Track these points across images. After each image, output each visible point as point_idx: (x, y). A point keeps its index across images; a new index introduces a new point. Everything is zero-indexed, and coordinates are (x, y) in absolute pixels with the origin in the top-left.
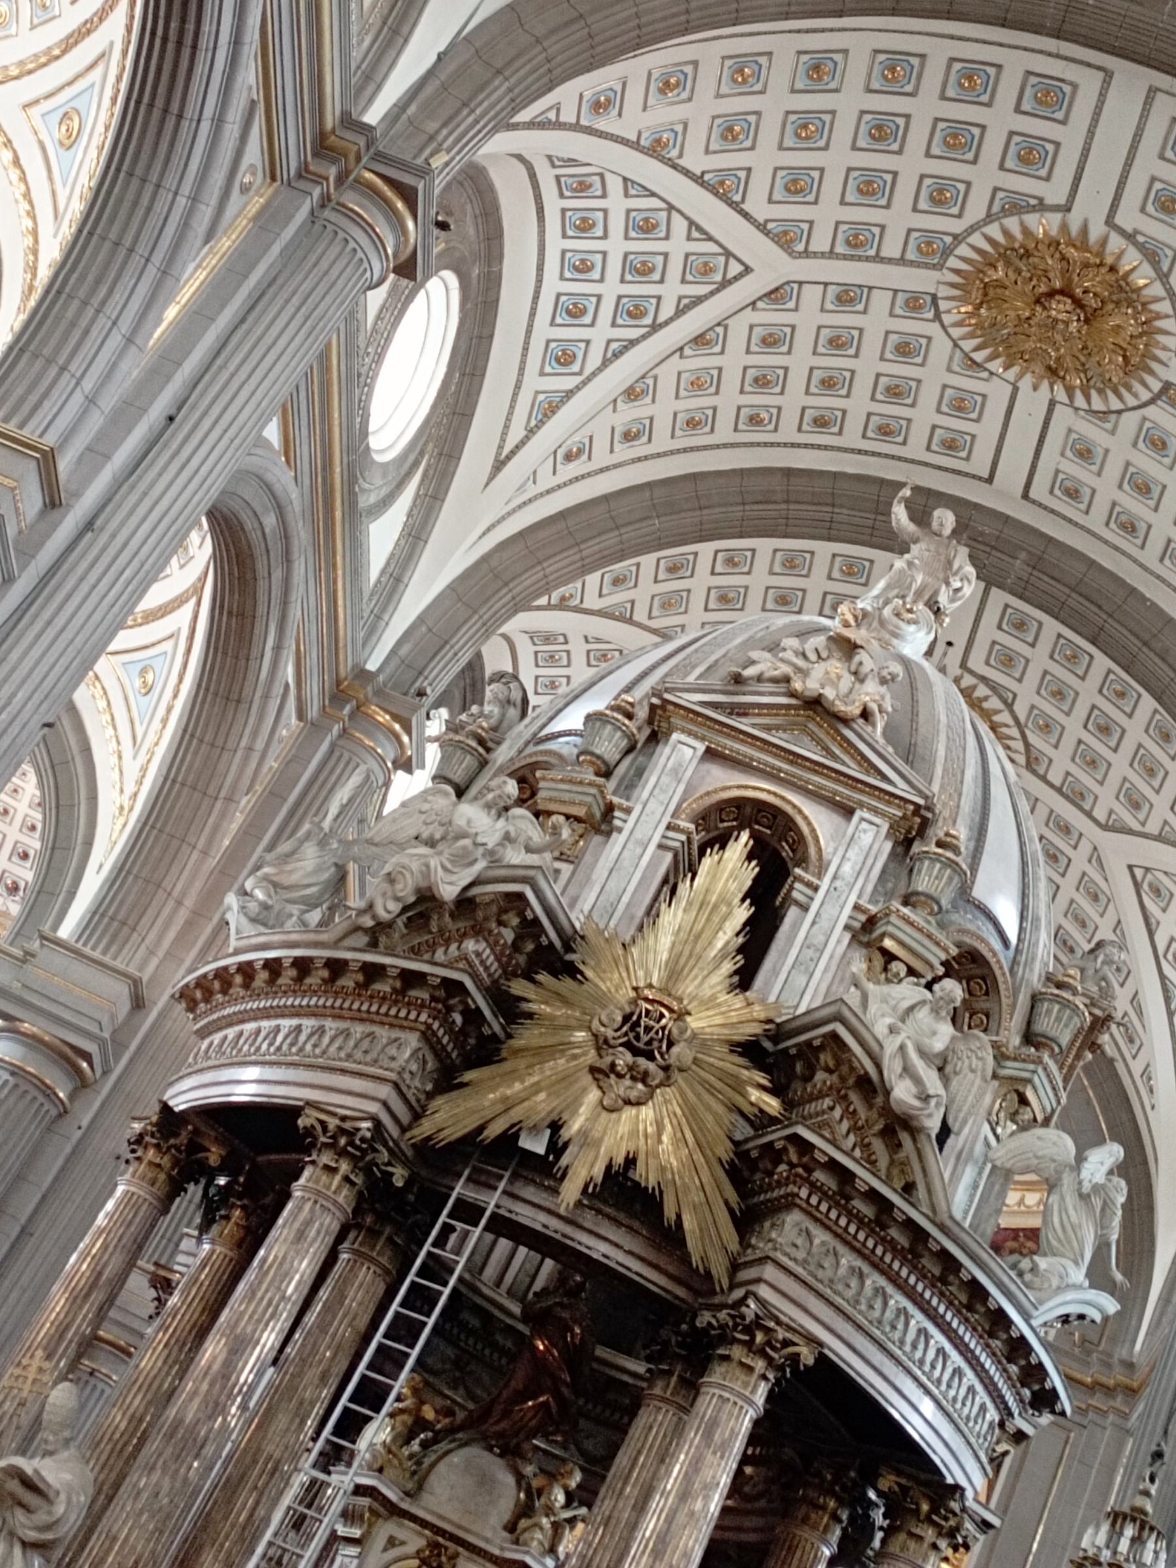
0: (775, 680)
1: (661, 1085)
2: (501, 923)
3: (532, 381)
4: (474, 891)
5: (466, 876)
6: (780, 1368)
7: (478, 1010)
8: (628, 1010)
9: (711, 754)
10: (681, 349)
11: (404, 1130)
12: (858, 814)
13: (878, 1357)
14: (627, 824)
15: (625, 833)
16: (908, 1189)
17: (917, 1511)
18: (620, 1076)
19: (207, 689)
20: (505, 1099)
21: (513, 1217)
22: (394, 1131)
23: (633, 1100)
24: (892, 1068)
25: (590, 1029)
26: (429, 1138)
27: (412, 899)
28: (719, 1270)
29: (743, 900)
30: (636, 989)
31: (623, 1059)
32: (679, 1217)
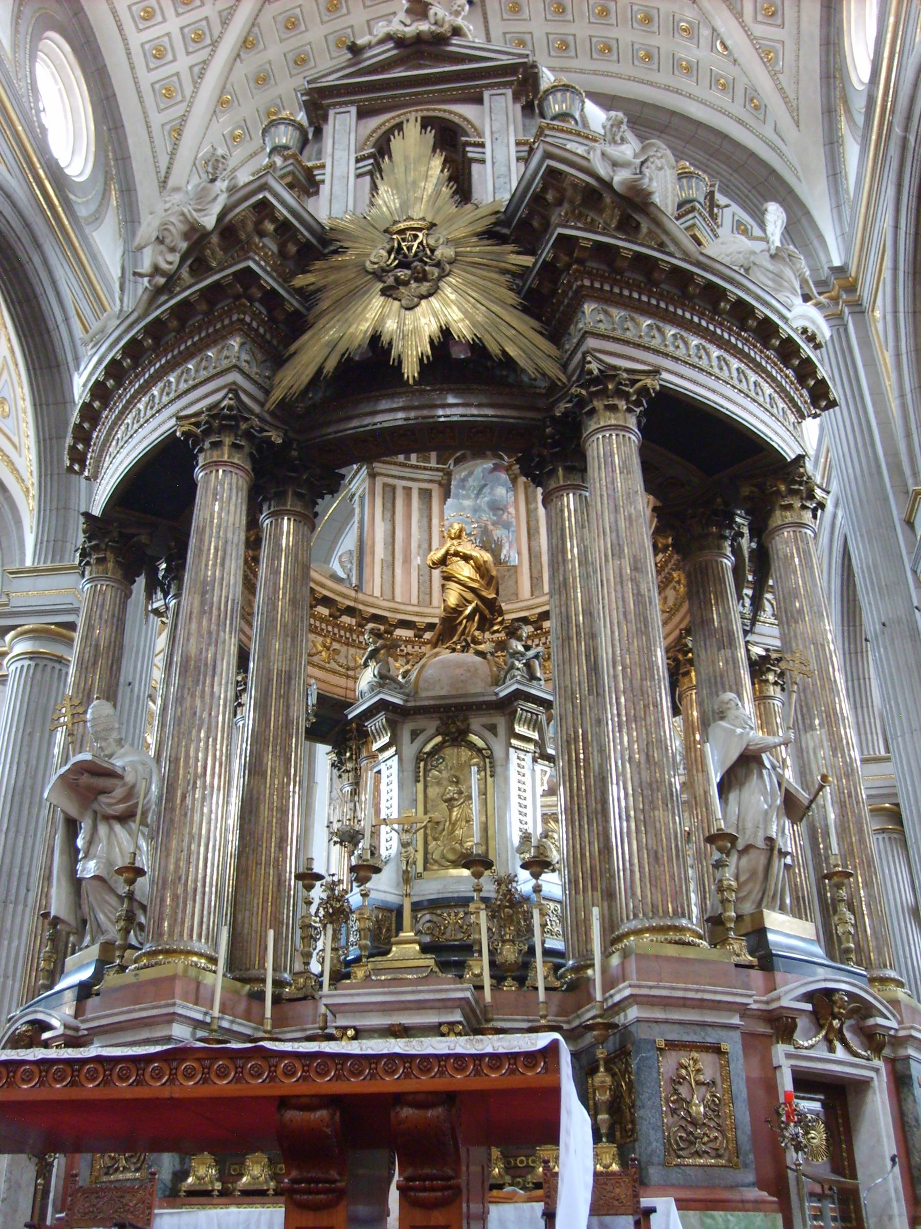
0: (381, 42)
1: (440, 278)
2: (262, 234)
3: (157, 119)
4: (230, 216)
5: (217, 208)
6: (638, 403)
8: (388, 247)
9: (363, 114)
10: (239, 55)
11: (262, 405)
12: (486, 95)
13: (702, 378)
14: (325, 175)
15: (328, 182)
16: (661, 247)
17: (778, 492)
18: (406, 284)
19: (34, 369)
20: (328, 344)
21: (379, 426)
22: (256, 408)
23: (425, 293)
24: (603, 170)
25: (367, 271)
26: (283, 399)
27: (184, 245)
28: (552, 370)
29: (434, 151)
30: (386, 231)
31: (403, 274)
32: (504, 353)
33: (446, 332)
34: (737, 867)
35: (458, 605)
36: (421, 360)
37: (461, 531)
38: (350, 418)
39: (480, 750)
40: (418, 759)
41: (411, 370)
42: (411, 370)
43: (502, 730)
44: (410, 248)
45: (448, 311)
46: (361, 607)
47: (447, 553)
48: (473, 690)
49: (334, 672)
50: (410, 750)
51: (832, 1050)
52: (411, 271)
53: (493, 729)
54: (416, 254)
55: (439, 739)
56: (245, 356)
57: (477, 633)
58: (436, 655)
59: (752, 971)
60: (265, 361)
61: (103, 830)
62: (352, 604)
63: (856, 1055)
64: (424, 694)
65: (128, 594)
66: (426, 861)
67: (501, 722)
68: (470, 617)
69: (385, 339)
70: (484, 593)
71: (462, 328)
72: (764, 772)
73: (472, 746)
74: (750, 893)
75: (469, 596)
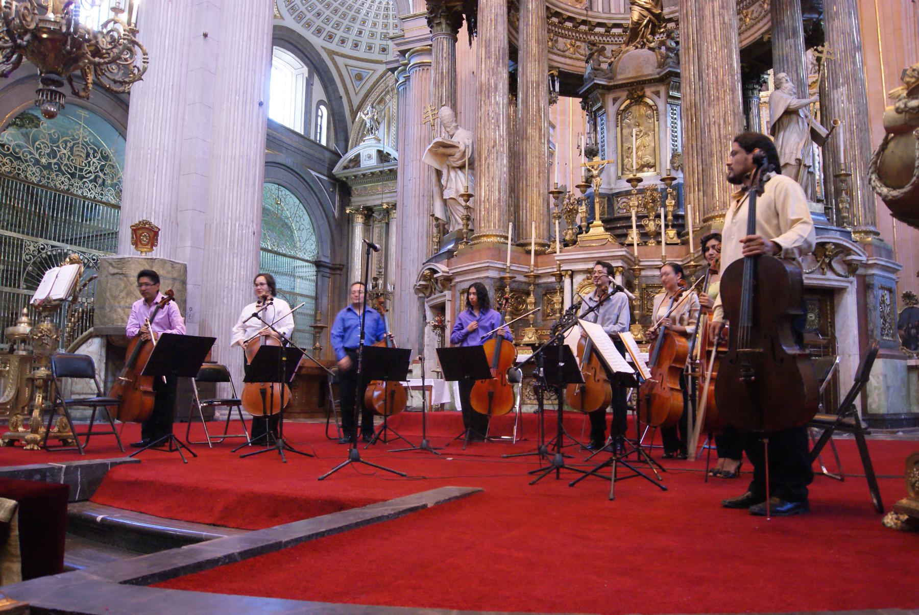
39: (651, 107)
40: (618, 114)
43: (663, 94)
46: (590, 19)
48: (646, 73)
49: (578, 59)
51: (824, 274)
53: (657, 93)
55: (628, 102)
57: (649, 37)
58: (627, 51)
61: (452, 174)
62: (585, 18)
63: (839, 275)
64: (619, 77)
65: (456, 40)
66: (623, 169)
67: (662, 89)
68: (646, 26)
70: (654, 11)
72: (800, 120)
73: (647, 104)
75: (645, 13)
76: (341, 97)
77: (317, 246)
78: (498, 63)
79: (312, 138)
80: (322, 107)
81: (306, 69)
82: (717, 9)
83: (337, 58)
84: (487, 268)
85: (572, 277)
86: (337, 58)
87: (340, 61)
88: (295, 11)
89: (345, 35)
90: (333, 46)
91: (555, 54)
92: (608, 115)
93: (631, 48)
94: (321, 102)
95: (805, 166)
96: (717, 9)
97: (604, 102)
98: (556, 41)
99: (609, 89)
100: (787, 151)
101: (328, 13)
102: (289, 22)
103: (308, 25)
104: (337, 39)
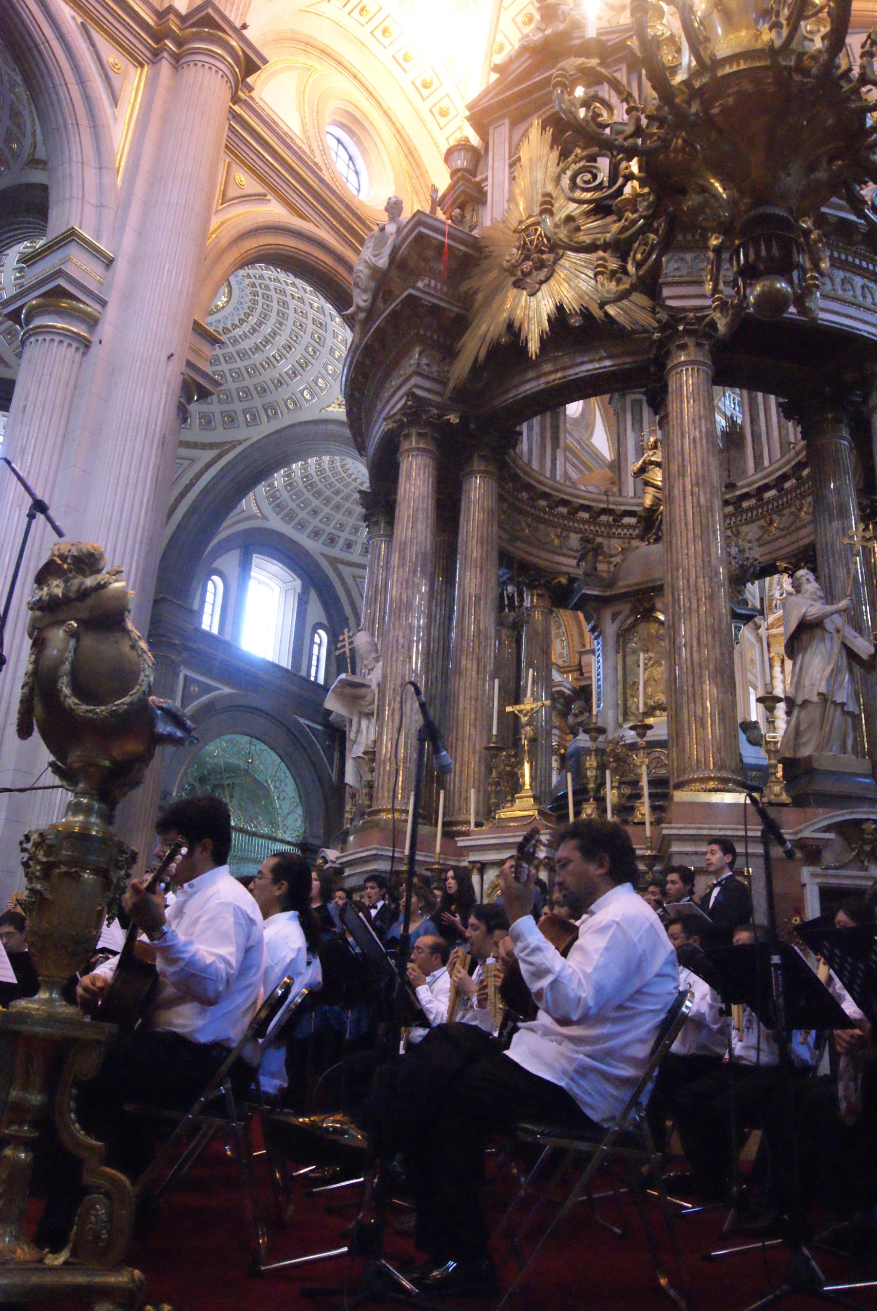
1: (555, 262)
7: (435, 307)
18: (529, 274)
22: (438, 399)
27: (372, 285)
29: (552, 148)
30: (515, 231)
33: (560, 308)
34: (798, 717)
35: (652, 505)
36: (541, 338)
37: (656, 442)
38: (509, 390)
41: (533, 346)
42: (533, 346)
44: (531, 242)
45: (574, 284)
46: (611, 507)
47: (644, 462)
50: (610, 628)
52: (538, 259)
54: (537, 246)
55: (632, 619)
56: (424, 361)
58: (637, 547)
59: (784, 809)
60: (444, 358)
62: (605, 506)
69: (517, 324)
71: (570, 301)
72: (827, 636)
74: (810, 739)
76: (347, 619)
77: (304, 821)
78: (415, 572)
79: (303, 673)
80: (321, 632)
81: (298, 583)
82: (688, 487)
83: (341, 567)
84: (375, 858)
85: (481, 873)
86: (341, 567)
87: (346, 571)
88: (282, 509)
89: (353, 538)
90: (336, 552)
91: (565, 555)
92: (604, 639)
93: (643, 545)
94: (319, 625)
95: (834, 703)
96: (688, 487)
97: (599, 618)
98: (567, 537)
99: (605, 601)
100: (807, 683)
101: (326, 510)
102: (276, 523)
103: (301, 526)
104: (341, 542)
